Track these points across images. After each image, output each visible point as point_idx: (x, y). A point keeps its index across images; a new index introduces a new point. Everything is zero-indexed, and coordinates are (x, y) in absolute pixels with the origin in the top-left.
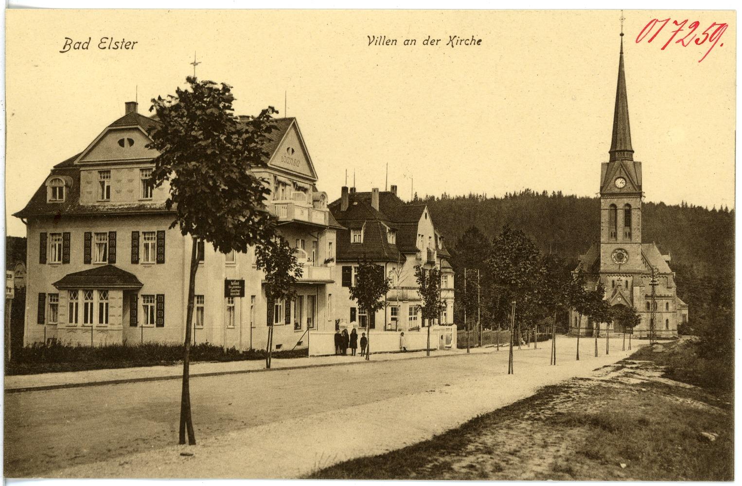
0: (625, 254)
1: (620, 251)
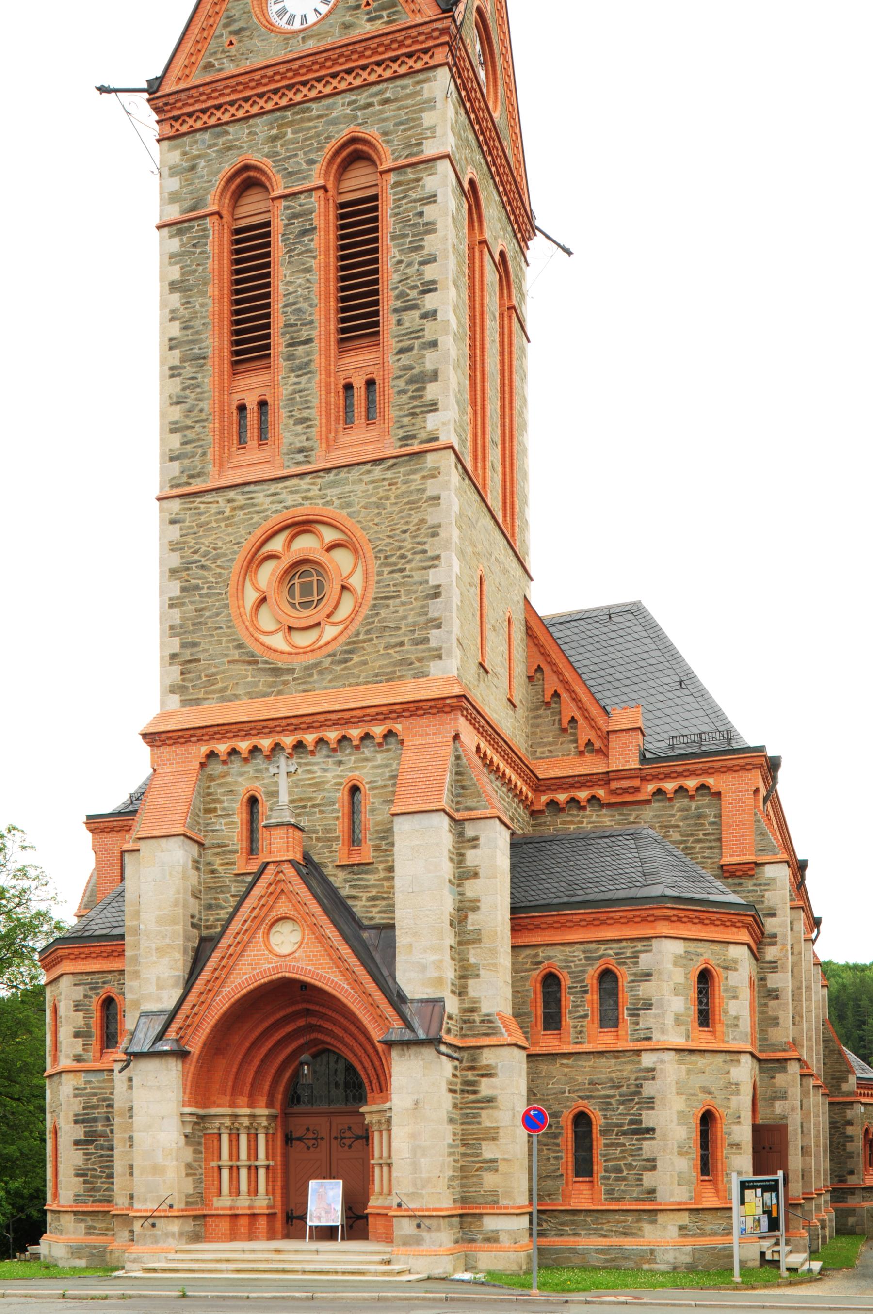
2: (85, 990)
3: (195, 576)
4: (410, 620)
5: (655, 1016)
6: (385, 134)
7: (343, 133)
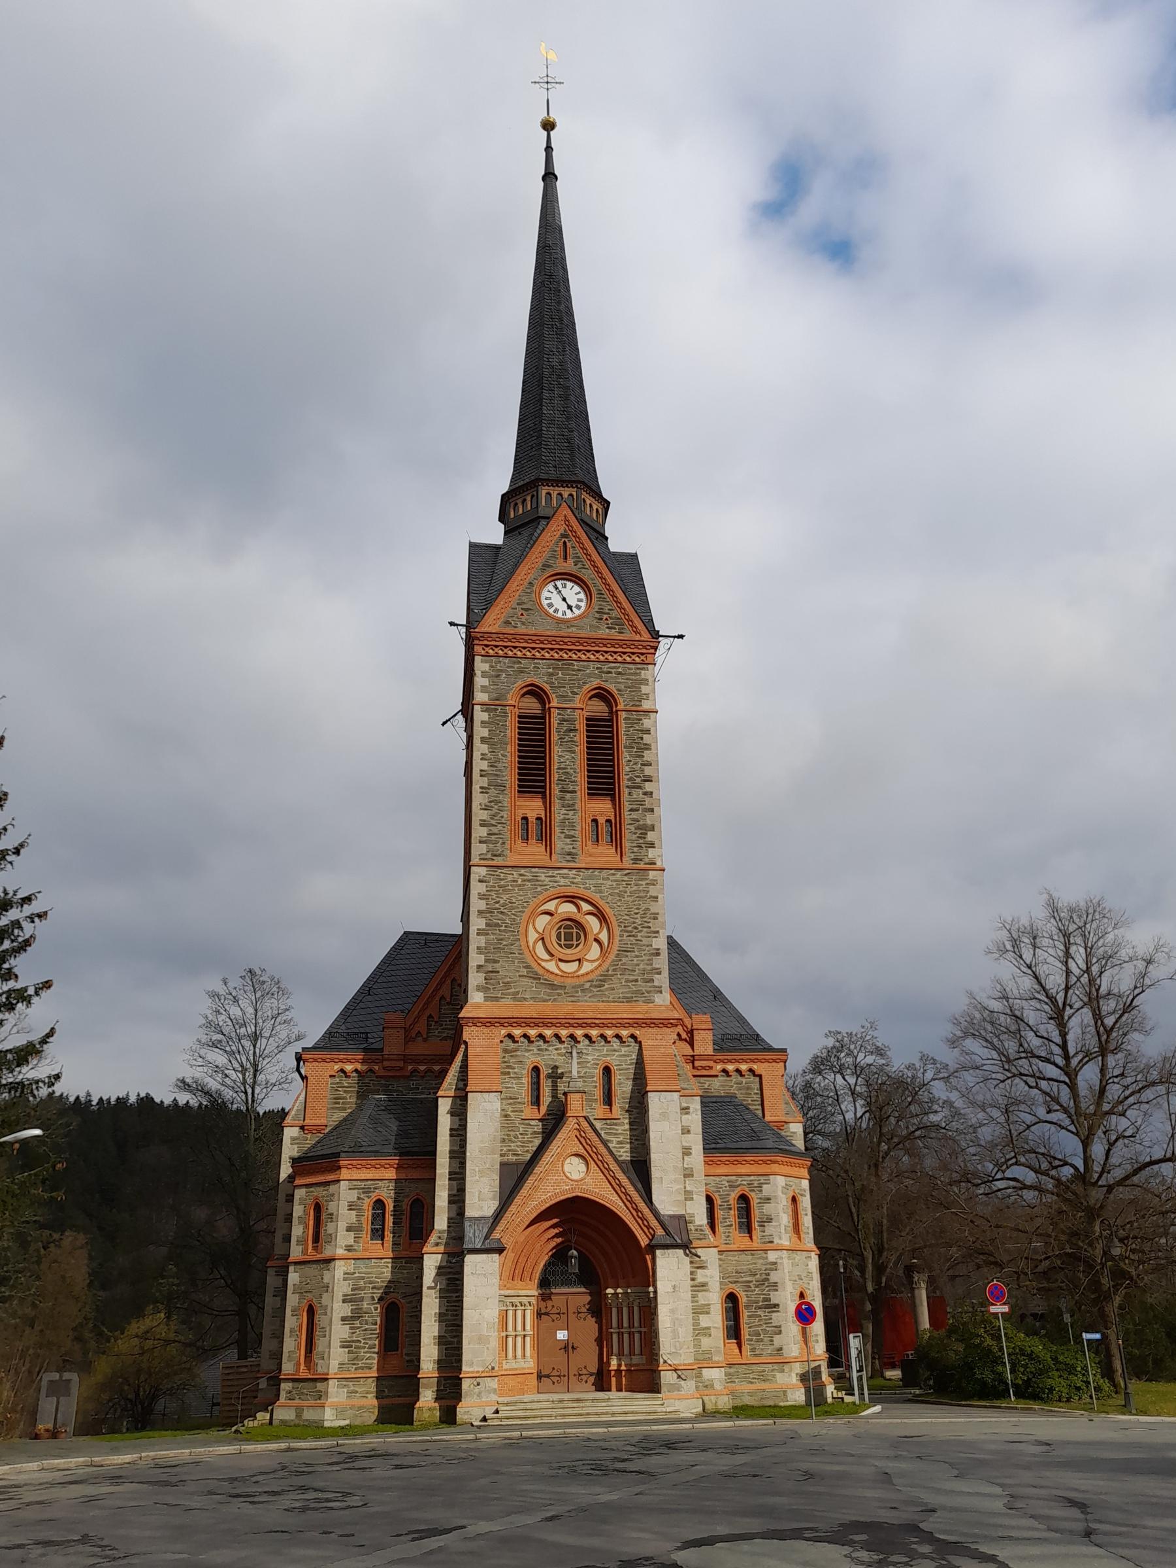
0: (593, 923)
1: (568, 908)
2: (359, 1193)
3: (496, 918)
4: (641, 966)
5: (775, 1227)
7: (596, 682)
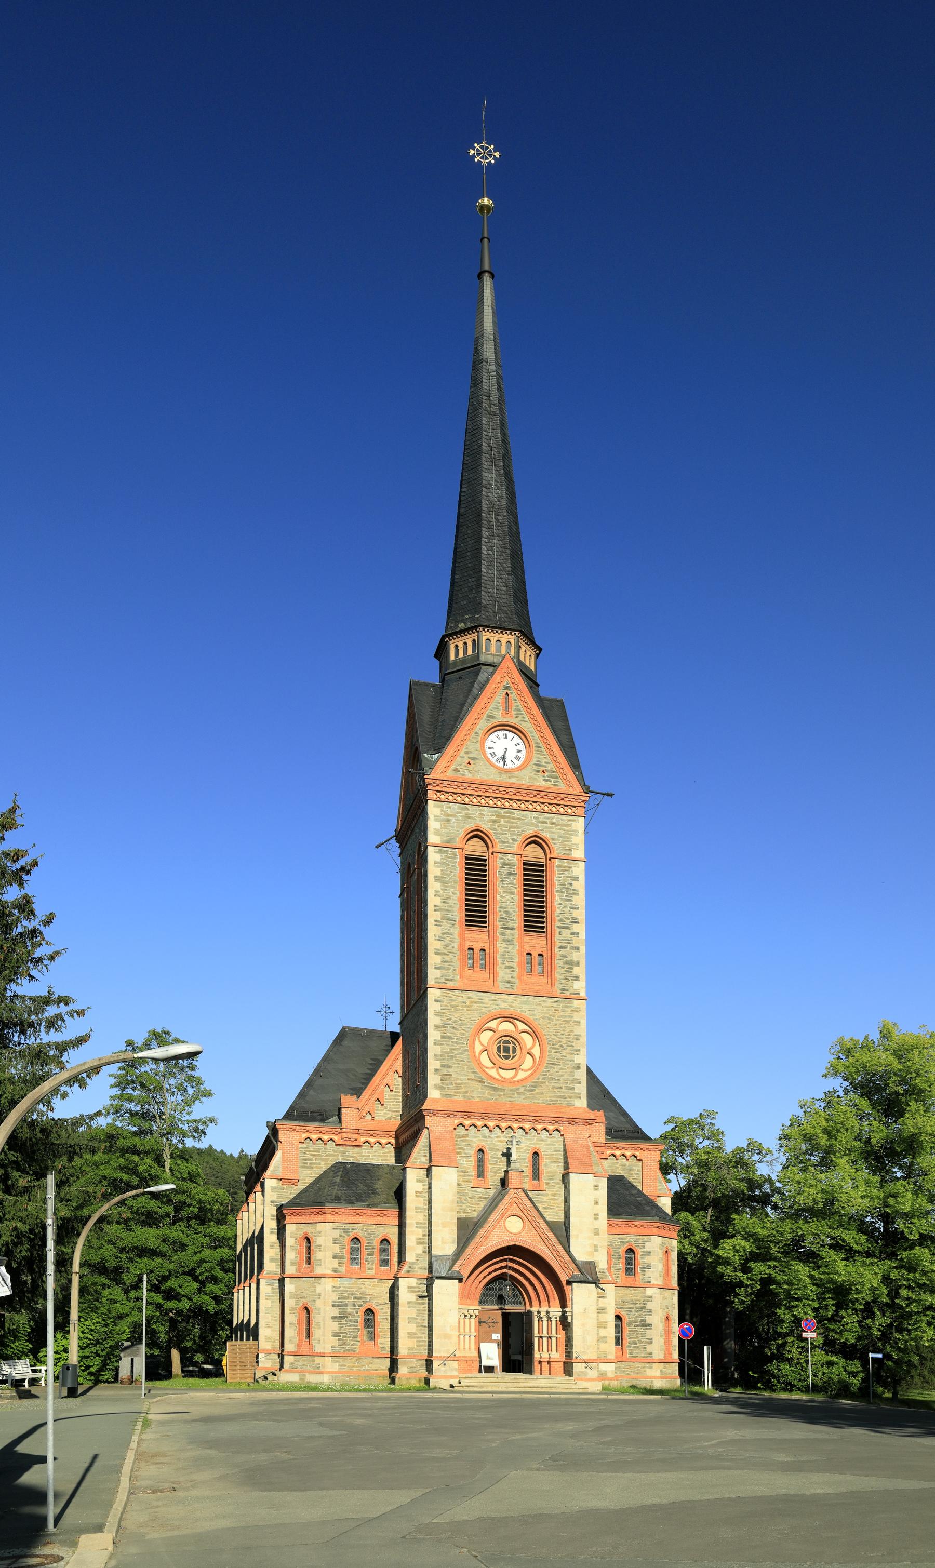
0: (527, 1039)
1: (507, 1027)
3: (449, 1031)
4: (565, 1077)
6: (553, 839)
7: (530, 831)
